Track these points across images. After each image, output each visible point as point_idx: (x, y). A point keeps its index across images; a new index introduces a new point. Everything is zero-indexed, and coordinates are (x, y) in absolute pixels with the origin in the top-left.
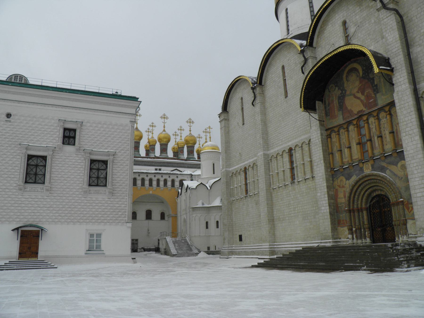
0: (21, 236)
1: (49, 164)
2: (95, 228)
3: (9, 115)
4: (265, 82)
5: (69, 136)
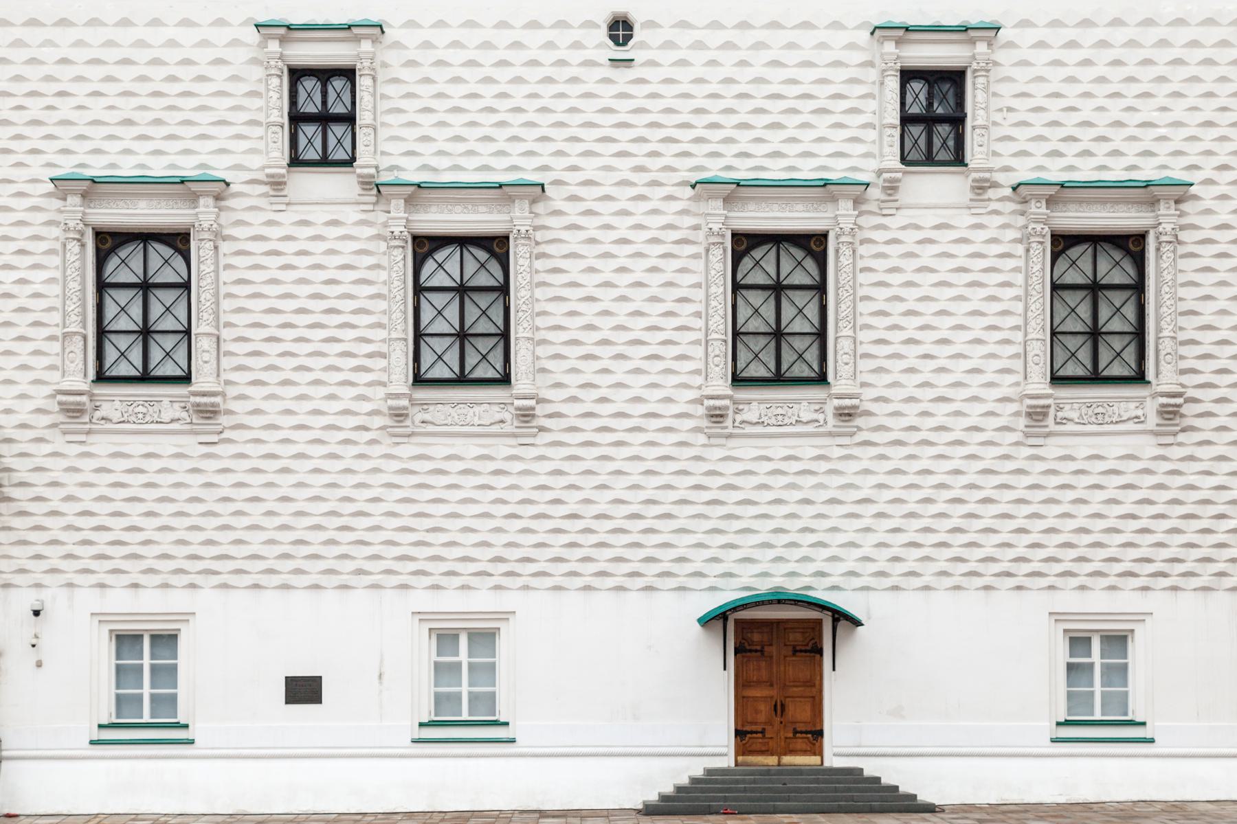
0: (737, 652)
1: (843, 278)
2: (1099, 604)
3: (620, 30)
5: (935, 113)
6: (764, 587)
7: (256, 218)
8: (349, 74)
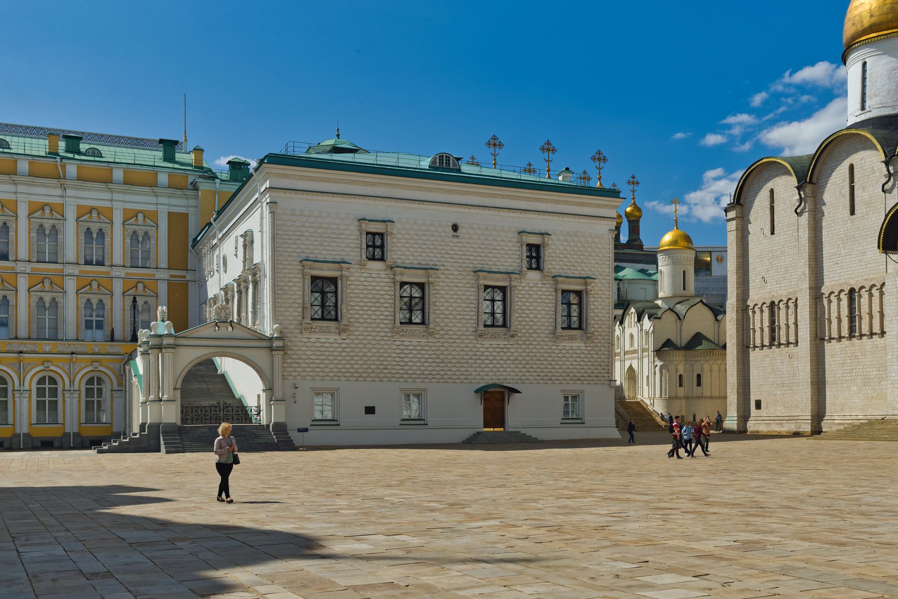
3: (455, 228)
4: (818, 180)
5: (535, 255)
6: (491, 382)
7: (357, 274)
8: (381, 235)
